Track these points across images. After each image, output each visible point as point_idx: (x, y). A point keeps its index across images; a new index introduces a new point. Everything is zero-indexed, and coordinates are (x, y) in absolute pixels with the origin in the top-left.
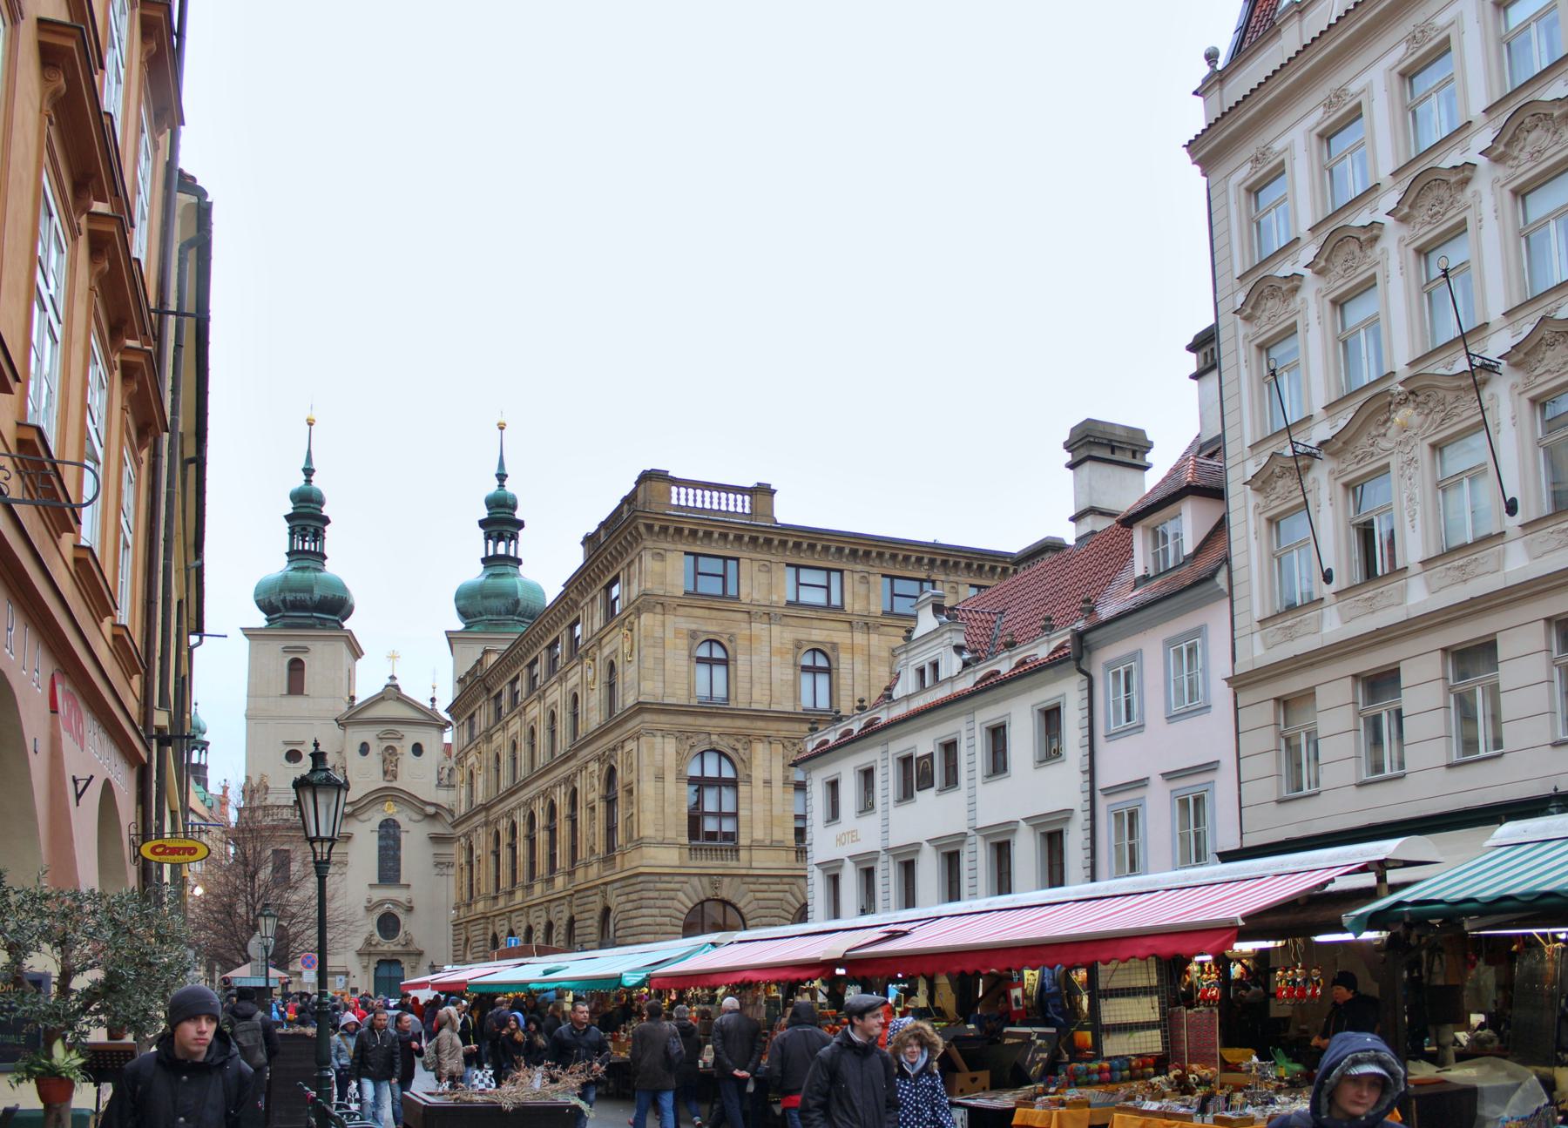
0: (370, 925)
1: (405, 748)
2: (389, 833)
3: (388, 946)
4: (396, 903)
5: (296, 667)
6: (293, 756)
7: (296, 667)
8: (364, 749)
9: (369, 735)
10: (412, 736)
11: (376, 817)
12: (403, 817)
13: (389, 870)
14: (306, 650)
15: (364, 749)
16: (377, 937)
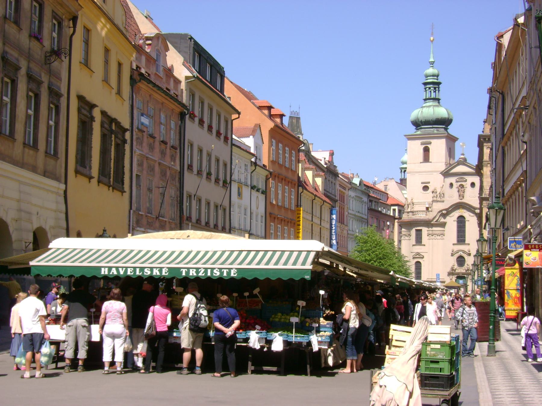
0: (453, 261)
1: (467, 185)
2: (461, 221)
3: (461, 270)
4: (464, 252)
5: (426, 150)
6: (426, 188)
7: (426, 150)
8: (451, 185)
9: (453, 180)
10: (470, 179)
11: (456, 214)
12: (466, 214)
13: (461, 238)
14: (430, 143)
15: (451, 185)
16: (456, 266)
